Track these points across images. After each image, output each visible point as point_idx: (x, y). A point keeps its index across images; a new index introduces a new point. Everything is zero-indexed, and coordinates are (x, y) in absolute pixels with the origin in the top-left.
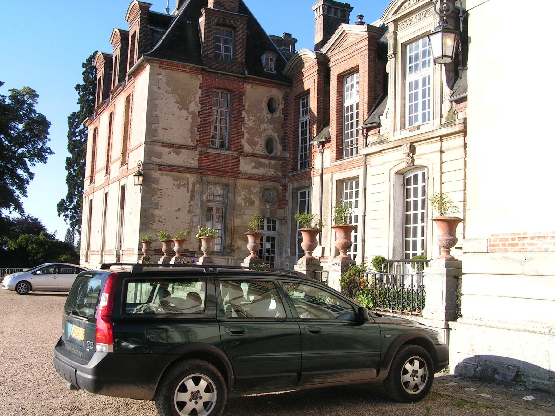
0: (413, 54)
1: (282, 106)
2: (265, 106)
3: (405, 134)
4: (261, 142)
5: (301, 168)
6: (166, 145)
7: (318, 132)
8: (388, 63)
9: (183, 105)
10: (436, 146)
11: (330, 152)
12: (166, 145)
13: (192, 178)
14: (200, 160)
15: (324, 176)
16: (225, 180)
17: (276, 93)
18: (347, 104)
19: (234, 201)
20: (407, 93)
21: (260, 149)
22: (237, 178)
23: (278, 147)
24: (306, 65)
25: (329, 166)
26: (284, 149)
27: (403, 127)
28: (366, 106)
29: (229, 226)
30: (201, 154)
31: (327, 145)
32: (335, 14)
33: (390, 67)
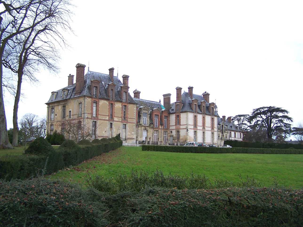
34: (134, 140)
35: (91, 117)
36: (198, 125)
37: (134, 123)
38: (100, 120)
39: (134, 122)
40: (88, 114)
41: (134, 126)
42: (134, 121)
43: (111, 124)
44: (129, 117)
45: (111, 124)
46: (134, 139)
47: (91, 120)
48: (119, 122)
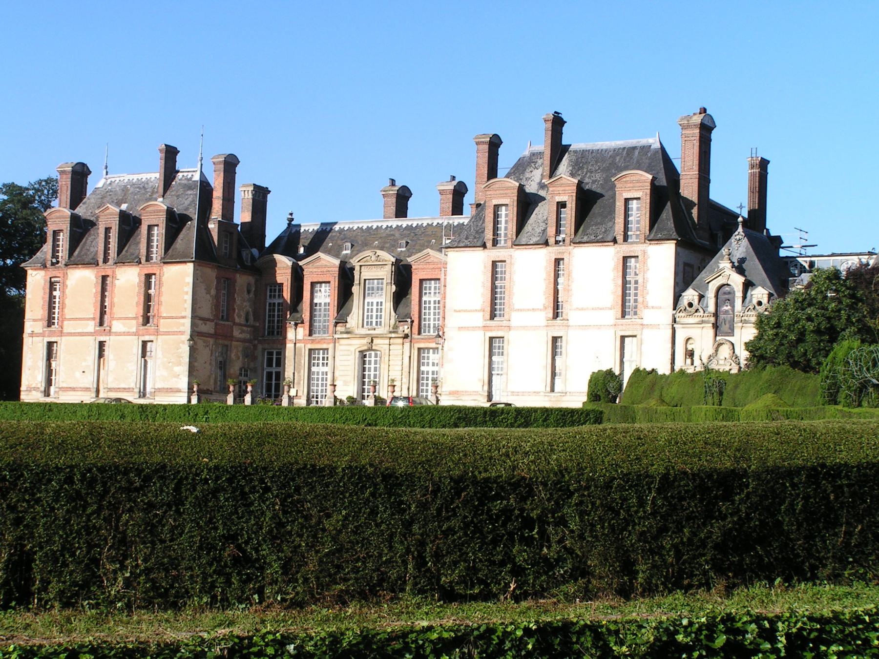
0: (371, 286)
1: (254, 289)
2: (245, 289)
4: (243, 314)
5: (269, 334)
6: (201, 319)
7: (290, 315)
8: (353, 288)
9: (208, 292)
10: (387, 341)
11: (302, 332)
12: (201, 319)
13: (211, 341)
14: (216, 328)
15: (297, 345)
16: (226, 342)
17: (251, 279)
18: (315, 301)
19: (230, 356)
20: (366, 307)
21: (243, 321)
22: (232, 340)
23: (251, 318)
24: (278, 265)
26: (254, 320)
27: (363, 326)
28: (336, 308)
29: (227, 374)
30: (216, 324)
31: (299, 325)
32: (259, 196)
33: (355, 289)
34: (181, 394)
35: (41, 331)
36: (516, 307)
37: (182, 333)
38: (70, 334)
39: (182, 329)
40: (34, 320)
41: (183, 342)
42: (183, 325)
43: (101, 344)
44: (165, 315)
45: (101, 344)
46: (179, 391)
47: (41, 338)
48: (128, 334)
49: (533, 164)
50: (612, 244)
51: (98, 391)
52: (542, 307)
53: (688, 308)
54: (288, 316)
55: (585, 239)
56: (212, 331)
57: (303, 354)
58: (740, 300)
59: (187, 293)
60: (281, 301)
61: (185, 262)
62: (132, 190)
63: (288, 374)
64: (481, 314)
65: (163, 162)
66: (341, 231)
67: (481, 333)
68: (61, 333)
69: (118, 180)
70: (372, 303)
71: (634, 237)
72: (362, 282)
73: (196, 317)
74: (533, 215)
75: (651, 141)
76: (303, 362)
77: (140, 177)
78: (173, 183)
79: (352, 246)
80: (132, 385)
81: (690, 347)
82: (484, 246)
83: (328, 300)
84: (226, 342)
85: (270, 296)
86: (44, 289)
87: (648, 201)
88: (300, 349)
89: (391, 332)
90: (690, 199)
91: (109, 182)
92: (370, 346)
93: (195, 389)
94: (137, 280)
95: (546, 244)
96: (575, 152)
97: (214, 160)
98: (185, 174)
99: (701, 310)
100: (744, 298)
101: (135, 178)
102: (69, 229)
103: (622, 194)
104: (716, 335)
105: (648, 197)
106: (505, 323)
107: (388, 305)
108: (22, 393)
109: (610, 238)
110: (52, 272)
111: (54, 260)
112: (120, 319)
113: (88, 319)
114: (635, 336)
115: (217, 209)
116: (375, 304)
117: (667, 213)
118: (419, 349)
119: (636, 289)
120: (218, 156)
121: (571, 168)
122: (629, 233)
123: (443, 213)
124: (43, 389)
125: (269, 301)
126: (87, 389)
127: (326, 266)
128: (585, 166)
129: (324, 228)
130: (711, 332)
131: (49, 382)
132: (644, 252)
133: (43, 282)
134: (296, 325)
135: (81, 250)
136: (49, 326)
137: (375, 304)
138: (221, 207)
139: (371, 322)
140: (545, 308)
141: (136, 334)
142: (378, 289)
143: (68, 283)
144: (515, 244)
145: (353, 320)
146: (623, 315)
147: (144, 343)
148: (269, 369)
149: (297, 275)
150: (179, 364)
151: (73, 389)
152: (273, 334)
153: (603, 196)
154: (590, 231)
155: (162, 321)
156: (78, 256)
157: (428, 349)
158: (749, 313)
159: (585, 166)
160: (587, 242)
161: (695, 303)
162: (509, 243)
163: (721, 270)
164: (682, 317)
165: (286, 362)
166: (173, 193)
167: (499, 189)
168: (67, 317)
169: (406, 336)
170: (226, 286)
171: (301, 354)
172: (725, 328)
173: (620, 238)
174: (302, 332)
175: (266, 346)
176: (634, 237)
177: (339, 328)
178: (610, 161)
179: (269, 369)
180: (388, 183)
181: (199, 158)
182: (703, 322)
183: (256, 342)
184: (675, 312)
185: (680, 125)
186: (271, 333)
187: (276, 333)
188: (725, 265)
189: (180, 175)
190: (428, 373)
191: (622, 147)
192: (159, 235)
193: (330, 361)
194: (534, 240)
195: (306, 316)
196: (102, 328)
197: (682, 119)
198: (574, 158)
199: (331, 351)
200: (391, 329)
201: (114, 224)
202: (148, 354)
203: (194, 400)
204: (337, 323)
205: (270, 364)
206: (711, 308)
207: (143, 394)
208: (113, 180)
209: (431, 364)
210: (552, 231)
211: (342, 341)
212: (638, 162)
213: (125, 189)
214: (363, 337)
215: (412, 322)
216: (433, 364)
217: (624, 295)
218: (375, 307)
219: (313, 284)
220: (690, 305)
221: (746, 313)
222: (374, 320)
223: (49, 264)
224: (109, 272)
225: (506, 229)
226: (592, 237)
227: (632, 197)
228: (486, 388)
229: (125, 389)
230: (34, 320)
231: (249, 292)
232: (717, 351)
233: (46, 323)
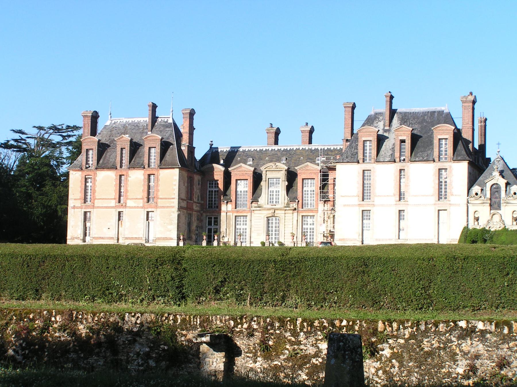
3: (269, 206)
5: (209, 207)
6: (182, 199)
10: (284, 212)
12: (182, 199)
13: (185, 211)
14: (187, 205)
15: (228, 214)
16: (191, 212)
18: (239, 189)
20: (269, 193)
22: (193, 211)
23: (200, 199)
24: (215, 170)
25: (230, 210)
26: (201, 200)
30: (187, 202)
31: (229, 203)
33: (263, 183)
35: (80, 205)
37: (173, 207)
38: (98, 207)
39: (172, 205)
40: (75, 199)
41: (173, 212)
42: (173, 203)
46: (171, 239)
47: (80, 210)
48: (138, 207)
49: (377, 119)
50: (432, 162)
51: (118, 239)
52: (392, 195)
53: (475, 196)
54: (222, 198)
55: (417, 159)
56: (186, 206)
57: (232, 219)
58: (505, 191)
59: (175, 185)
60: (216, 189)
61: (174, 168)
62: (129, 127)
63: (223, 228)
64: (357, 198)
65: (151, 112)
66: (244, 151)
67: (358, 208)
68: (93, 207)
69: (119, 121)
70: (273, 191)
71: (443, 159)
72: (267, 179)
73: (180, 198)
74: (383, 146)
75: (443, 108)
76: (231, 223)
77: (133, 120)
78: (156, 124)
79: (253, 159)
80: (141, 236)
81: (477, 216)
82: (358, 162)
83: (246, 189)
84: (191, 212)
85: (210, 187)
86: (81, 182)
87: (452, 140)
88: (230, 216)
89: (285, 207)
90: (468, 139)
91: (113, 122)
92: (273, 214)
93: (181, 238)
94: (142, 177)
95: (395, 162)
96: (400, 113)
97: (183, 112)
98: (163, 119)
99: (483, 197)
100: (506, 191)
101: (130, 120)
102: (97, 148)
103: (437, 136)
104: (491, 210)
105: (452, 138)
106: (371, 203)
107: (283, 192)
108: (68, 240)
109: (431, 159)
110: (86, 173)
111: (87, 166)
112: (132, 199)
113: (112, 199)
114: (446, 210)
115: (186, 139)
116: (275, 192)
117: (460, 146)
118: (302, 216)
119: (446, 185)
120: (186, 109)
121: (400, 122)
122: (441, 157)
123: (303, 143)
124: (82, 238)
125: (209, 189)
126: (112, 238)
127: (245, 171)
128: (408, 121)
129: (233, 150)
130: (489, 208)
131: (85, 235)
132: (450, 167)
133: (80, 178)
134: (227, 203)
135: (104, 160)
136: (85, 203)
137: (275, 192)
138: (188, 138)
139: (273, 202)
140: (394, 195)
141: (143, 207)
142: (276, 183)
143: (97, 178)
144: (377, 161)
145: (263, 200)
146: (439, 198)
147: (148, 213)
148: (210, 227)
149: (227, 176)
150: (171, 224)
151: (102, 238)
152: (212, 207)
153: (422, 137)
154: (418, 155)
155: (159, 200)
156: (103, 163)
157: (307, 216)
158: (509, 198)
159: (408, 121)
160: (419, 161)
161: (479, 193)
162: (373, 161)
163: (494, 176)
164: (472, 200)
165: (221, 223)
166: (157, 129)
167: (366, 132)
168: (97, 198)
169: (295, 209)
170: (190, 180)
171: (230, 219)
172: (496, 206)
173: (437, 159)
174: (230, 207)
175: (208, 214)
176: (443, 159)
177: (254, 205)
178: (422, 118)
179: (210, 227)
180: (269, 126)
181: (171, 110)
182: (483, 203)
183: (202, 212)
184: (468, 198)
185: (462, 101)
186: (210, 207)
187: (213, 207)
188: (496, 174)
189: (159, 120)
190: (307, 229)
191: (427, 111)
192: (155, 153)
193: (248, 223)
194: (387, 159)
195: (233, 198)
196: (120, 204)
197: (462, 98)
198: (400, 116)
199: (248, 218)
200: (285, 205)
201: (127, 145)
202: (150, 219)
203: (181, 244)
204: (252, 202)
205: (210, 223)
206: (488, 196)
207: (147, 241)
208: (116, 121)
209: (309, 224)
210: (397, 154)
211: (255, 212)
212: (438, 119)
213: (124, 126)
214: (269, 209)
215: (298, 201)
216: (311, 224)
217: (440, 188)
218: (275, 193)
219: (237, 180)
220: (477, 194)
221: (508, 198)
222: (274, 200)
223: (84, 168)
224: (124, 173)
225: (370, 153)
226: (421, 158)
227: (443, 138)
228: (361, 237)
229: (136, 238)
230: (75, 199)
231: (199, 184)
232: (492, 218)
233: (83, 201)
